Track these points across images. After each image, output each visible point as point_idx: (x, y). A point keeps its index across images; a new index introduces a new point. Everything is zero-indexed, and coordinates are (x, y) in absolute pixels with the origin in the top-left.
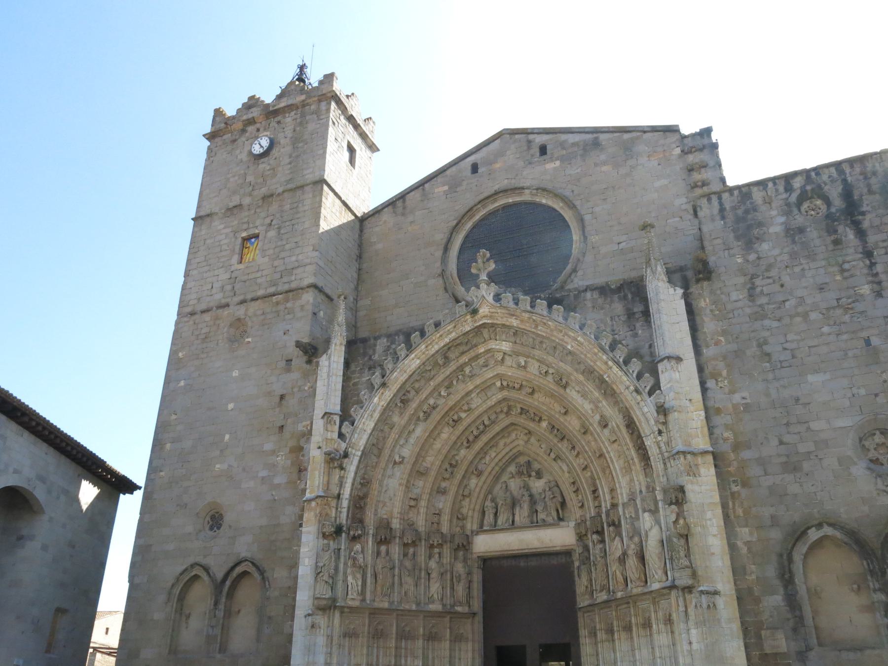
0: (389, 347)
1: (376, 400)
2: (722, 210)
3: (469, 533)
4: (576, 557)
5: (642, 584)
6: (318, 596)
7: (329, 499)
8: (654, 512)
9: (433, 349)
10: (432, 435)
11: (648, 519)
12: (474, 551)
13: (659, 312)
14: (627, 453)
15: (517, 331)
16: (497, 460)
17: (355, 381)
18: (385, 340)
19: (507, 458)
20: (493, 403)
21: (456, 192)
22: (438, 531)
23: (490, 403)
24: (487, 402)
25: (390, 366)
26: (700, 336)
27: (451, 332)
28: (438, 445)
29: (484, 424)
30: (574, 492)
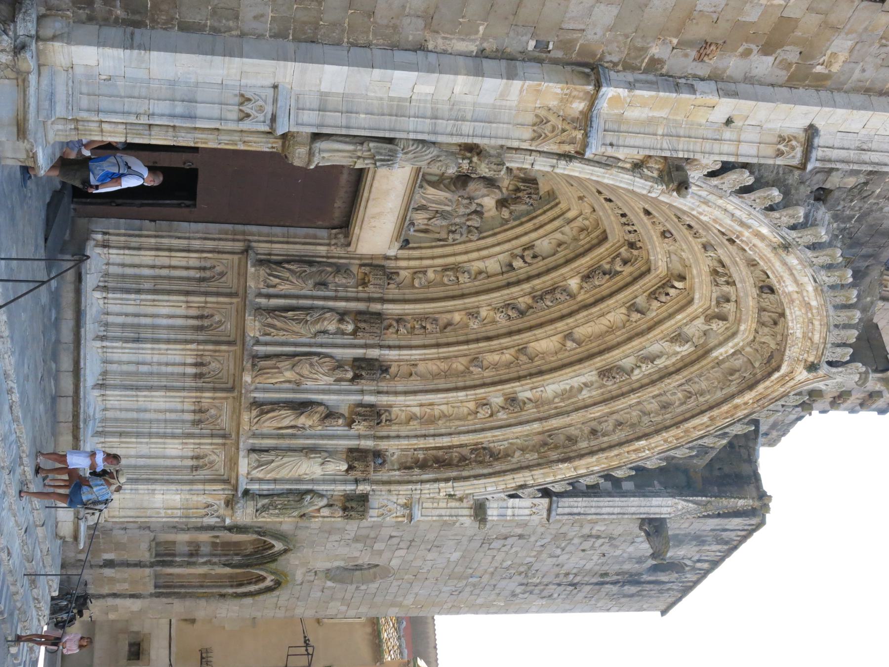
29: (625, 224)
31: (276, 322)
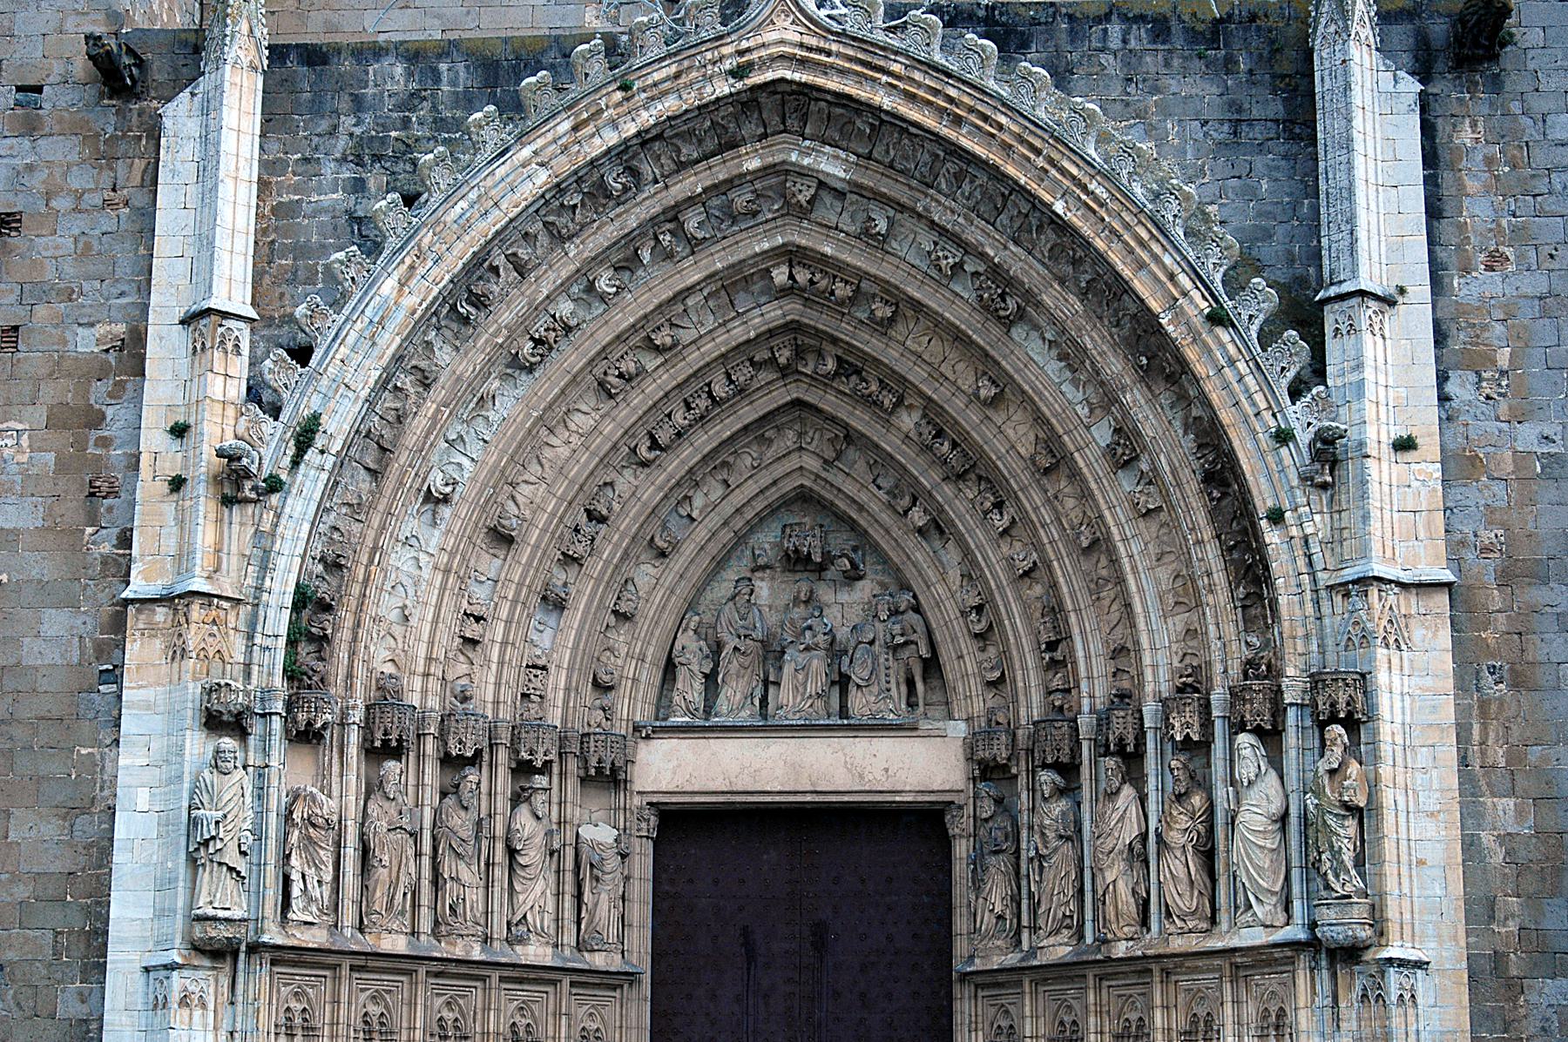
1: (388, 286)
3: (622, 728)
4: (960, 825)
5: (1204, 925)
6: (210, 912)
7: (225, 605)
8: (1270, 737)
9: (597, 141)
10: (550, 419)
11: (1247, 752)
12: (637, 787)
13: (1348, 145)
14: (1196, 553)
15: (882, 122)
16: (727, 508)
17: (285, 198)
18: (399, 70)
19: (759, 505)
20: (752, 334)
22: (539, 725)
23: (739, 333)
24: (730, 326)
25: (441, 179)
26: (1445, 228)
27: (665, 93)
28: (559, 448)
29: (710, 394)
30: (976, 635)
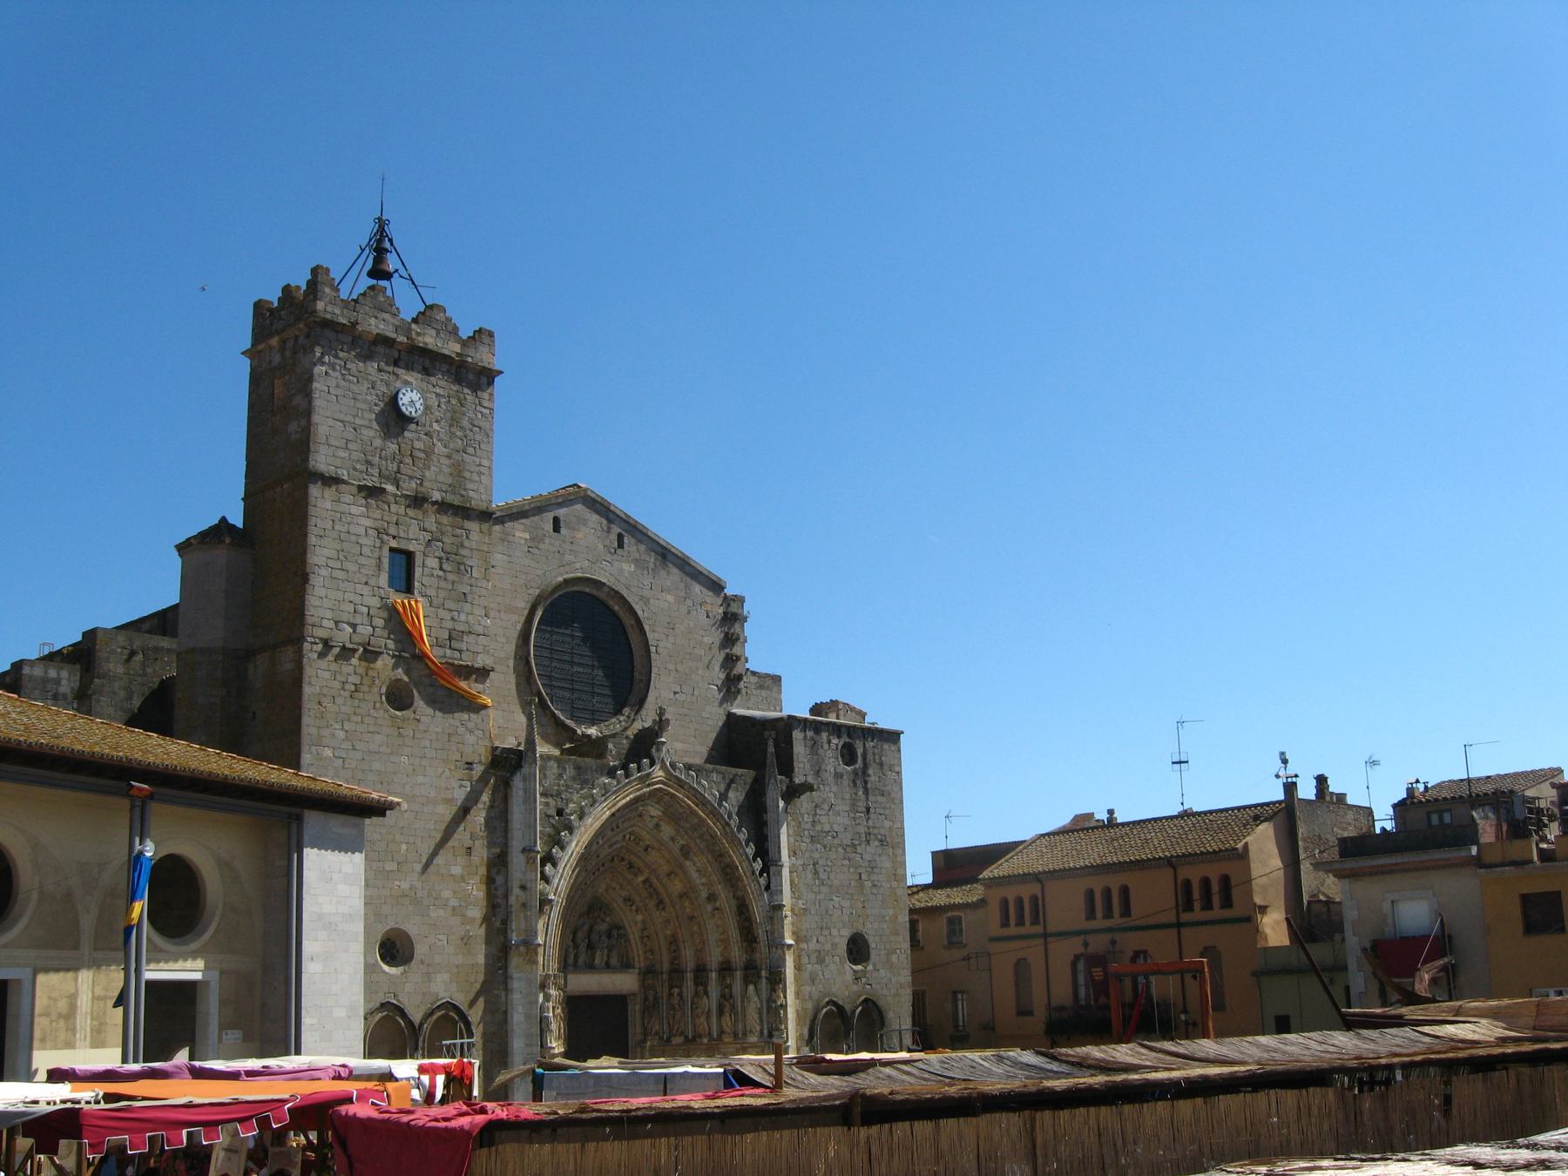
0: (560, 776)
2: (805, 737)
18: (555, 765)
21: (538, 548)
31: (676, 1028)
